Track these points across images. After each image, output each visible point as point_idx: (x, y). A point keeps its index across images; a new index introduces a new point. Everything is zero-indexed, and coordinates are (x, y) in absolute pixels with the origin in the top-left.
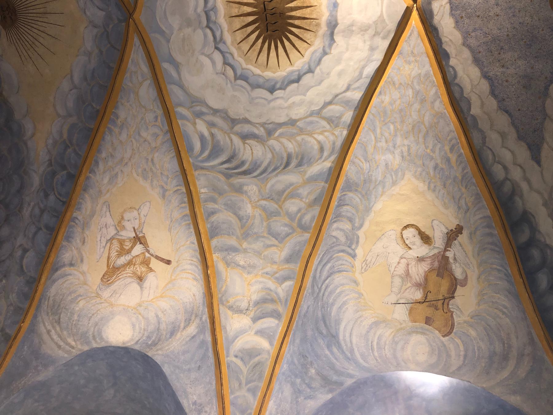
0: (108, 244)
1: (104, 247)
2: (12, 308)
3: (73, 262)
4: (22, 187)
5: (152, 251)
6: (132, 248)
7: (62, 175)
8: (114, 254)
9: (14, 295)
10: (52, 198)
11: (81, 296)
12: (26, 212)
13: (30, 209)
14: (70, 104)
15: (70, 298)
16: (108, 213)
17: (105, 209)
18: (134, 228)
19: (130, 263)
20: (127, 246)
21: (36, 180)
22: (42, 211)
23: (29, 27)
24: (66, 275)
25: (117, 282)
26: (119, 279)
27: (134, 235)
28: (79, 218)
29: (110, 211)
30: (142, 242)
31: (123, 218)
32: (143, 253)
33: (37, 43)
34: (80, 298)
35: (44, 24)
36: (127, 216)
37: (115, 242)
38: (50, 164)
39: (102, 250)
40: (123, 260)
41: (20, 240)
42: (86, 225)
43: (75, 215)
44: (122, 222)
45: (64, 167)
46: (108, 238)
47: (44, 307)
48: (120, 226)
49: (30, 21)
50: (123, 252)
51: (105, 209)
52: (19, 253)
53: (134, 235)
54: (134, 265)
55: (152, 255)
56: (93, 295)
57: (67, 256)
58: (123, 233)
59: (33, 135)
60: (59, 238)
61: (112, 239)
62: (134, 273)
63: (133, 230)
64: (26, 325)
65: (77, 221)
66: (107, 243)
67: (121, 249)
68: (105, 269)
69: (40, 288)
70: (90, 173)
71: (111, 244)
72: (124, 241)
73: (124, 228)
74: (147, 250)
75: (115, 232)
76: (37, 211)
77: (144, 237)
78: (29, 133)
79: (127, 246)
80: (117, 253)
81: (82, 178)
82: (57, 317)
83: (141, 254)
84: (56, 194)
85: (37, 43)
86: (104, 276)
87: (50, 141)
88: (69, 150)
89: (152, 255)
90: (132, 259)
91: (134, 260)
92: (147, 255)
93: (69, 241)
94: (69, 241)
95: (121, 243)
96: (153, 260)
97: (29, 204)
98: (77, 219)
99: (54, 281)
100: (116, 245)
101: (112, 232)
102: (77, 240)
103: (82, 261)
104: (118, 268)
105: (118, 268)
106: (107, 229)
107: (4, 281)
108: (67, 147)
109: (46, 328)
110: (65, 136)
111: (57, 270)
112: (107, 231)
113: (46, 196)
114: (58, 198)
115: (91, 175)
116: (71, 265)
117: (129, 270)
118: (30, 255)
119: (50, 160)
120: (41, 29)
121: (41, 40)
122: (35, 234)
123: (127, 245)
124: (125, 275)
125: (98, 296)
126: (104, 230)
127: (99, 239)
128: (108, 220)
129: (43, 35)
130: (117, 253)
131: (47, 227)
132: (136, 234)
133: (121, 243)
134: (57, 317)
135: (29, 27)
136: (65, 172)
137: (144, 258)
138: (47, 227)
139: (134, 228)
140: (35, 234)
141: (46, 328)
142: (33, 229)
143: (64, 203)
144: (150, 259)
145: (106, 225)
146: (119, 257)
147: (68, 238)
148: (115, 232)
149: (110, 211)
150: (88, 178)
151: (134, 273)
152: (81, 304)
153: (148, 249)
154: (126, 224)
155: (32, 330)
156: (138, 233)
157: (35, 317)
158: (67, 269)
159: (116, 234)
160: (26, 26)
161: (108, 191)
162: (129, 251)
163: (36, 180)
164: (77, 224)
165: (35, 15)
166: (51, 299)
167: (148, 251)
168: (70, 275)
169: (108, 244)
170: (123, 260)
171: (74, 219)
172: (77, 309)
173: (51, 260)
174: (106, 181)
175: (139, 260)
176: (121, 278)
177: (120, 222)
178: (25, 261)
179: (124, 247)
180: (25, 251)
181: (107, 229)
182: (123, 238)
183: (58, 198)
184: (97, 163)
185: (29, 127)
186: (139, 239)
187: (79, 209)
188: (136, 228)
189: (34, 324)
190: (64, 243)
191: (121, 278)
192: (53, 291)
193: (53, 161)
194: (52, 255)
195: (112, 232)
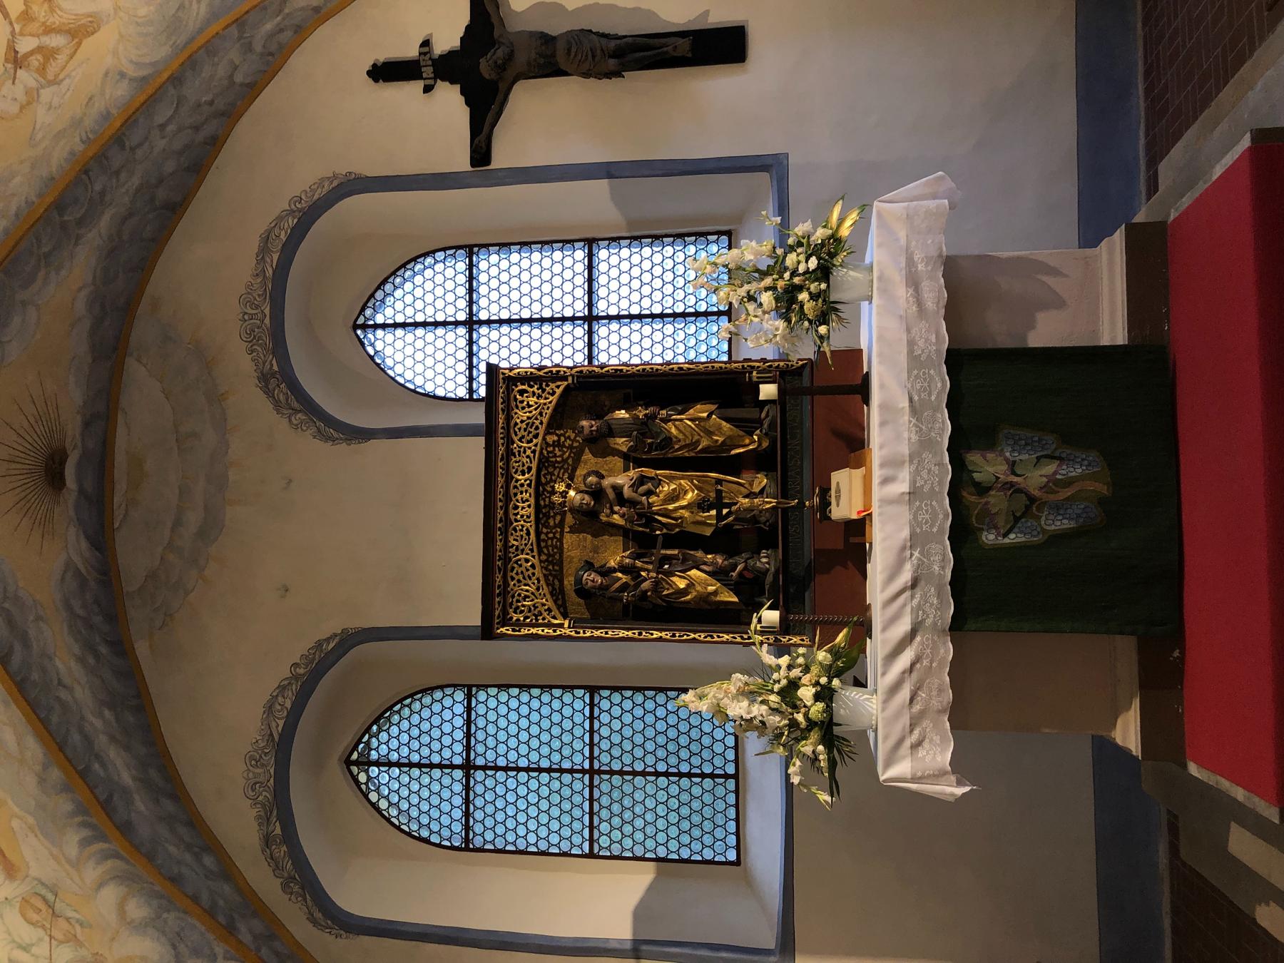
0: (61, 77)
1: (68, 76)
2: (216, 59)
3: (118, 77)
4: (125, 220)
5: (8, 29)
6: (32, 53)
7: (70, 216)
8: (62, 58)
9: (203, 75)
10: (98, 187)
11: (137, 22)
12: (136, 181)
13: (130, 184)
14: (16, 321)
15: (151, 29)
16: (38, 127)
17: (39, 136)
18: (13, 83)
19: (49, 30)
20: (38, 60)
21: (105, 222)
22: (117, 173)
23: (36, 445)
24: (136, 64)
25: (80, 12)
26: (76, 15)
27: (19, 71)
28: (79, 139)
29: (34, 128)
30: (13, 54)
31: (22, 108)
32: (22, 34)
33: (32, 421)
34: (139, 20)
35: (16, 446)
36: (15, 109)
37: (50, 77)
38: (78, 237)
39: (74, 74)
40: (56, 41)
41: (161, 144)
42: (76, 123)
43: (81, 147)
44: (24, 103)
45: (64, 226)
46: (56, 86)
47: (183, 39)
48: (32, 97)
49: (32, 454)
50: (48, 54)
51: (39, 136)
52: (170, 128)
53: (19, 71)
54: (44, 23)
55: (11, 23)
56: (122, 14)
57: (121, 91)
58: (32, 83)
59: (80, 289)
60: (118, 124)
61: (51, 83)
62: (52, 10)
63: (17, 81)
64: (216, 28)
65: (84, 138)
66: (62, 81)
67: (49, 59)
68: (88, 43)
69: (175, 65)
70: (33, 203)
71: (57, 76)
72: (38, 71)
73: (28, 92)
74: (13, 36)
75: (42, 91)
76: (123, 175)
77: (7, 60)
78: (84, 293)
79: (38, 60)
80: (57, 56)
81: (50, 199)
82: (180, 14)
83: (25, 35)
84: (90, 191)
85: (32, 421)
86: (93, 34)
87: (63, 272)
88: (45, 249)
89: (11, 23)
90: (42, 34)
91: (41, 31)
92: (17, 28)
93: (108, 113)
94: (108, 113)
95: (42, 70)
96: (13, 16)
97: (128, 190)
98: (81, 140)
99: (153, 64)
100: (52, 70)
101: (46, 94)
102: (99, 106)
103: (106, 74)
104: (69, 32)
105: (69, 32)
106: (51, 103)
107: (204, 99)
108: (47, 256)
109: (199, 8)
110: (41, 274)
111: (144, 79)
112: (52, 99)
113: (103, 193)
114: (91, 182)
115: (34, 199)
116: (122, 75)
117: (55, 20)
118: (160, 119)
119: (76, 244)
120: (20, 440)
121: (26, 424)
122: (140, 145)
123: (35, 61)
124: (65, 15)
125: (117, 9)
126: (56, 101)
127: (68, 94)
128: (42, 116)
129: (22, 432)
130: (57, 56)
131: (123, 147)
132: (16, 71)
133: (42, 70)
134: (180, 14)
135: (36, 445)
136: (66, 218)
137: (24, 25)
138: (123, 147)
139: (13, 83)
140: (140, 145)
141: (199, 8)
142: (139, 153)
143: (86, 172)
144: (18, 18)
145: (49, 109)
146: (58, 49)
147: (106, 116)
148: (42, 91)
149: (34, 128)
150: (40, 196)
151: (52, 10)
152: (143, 11)
153: (11, 37)
154: (21, 97)
155: (213, 16)
156: (12, 71)
157: (201, 31)
158: (132, 72)
159: (42, 87)
160: (38, 448)
161: (22, 162)
162: (39, 49)
163: (105, 222)
164: (86, 133)
165: (23, 461)
166: (171, 43)
167: (13, 33)
168: (131, 61)
169: (61, 77)
170: (56, 41)
171: (87, 141)
172: (152, 8)
173: (143, 98)
174: (17, 180)
175: (34, 27)
176: (72, 14)
177: (29, 103)
178: (171, 113)
179: (42, 60)
180: (162, 127)
181: (51, 103)
182: (36, 75)
183: (91, 182)
184: (17, 215)
185: (81, 306)
186: (16, 61)
187: (72, 153)
188: (11, 82)
189: (207, 23)
190: (114, 111)
191: (72, 14)
192: (163, 52)
193: (73, 241)
194: (137, 104)
195: (46, 94)
